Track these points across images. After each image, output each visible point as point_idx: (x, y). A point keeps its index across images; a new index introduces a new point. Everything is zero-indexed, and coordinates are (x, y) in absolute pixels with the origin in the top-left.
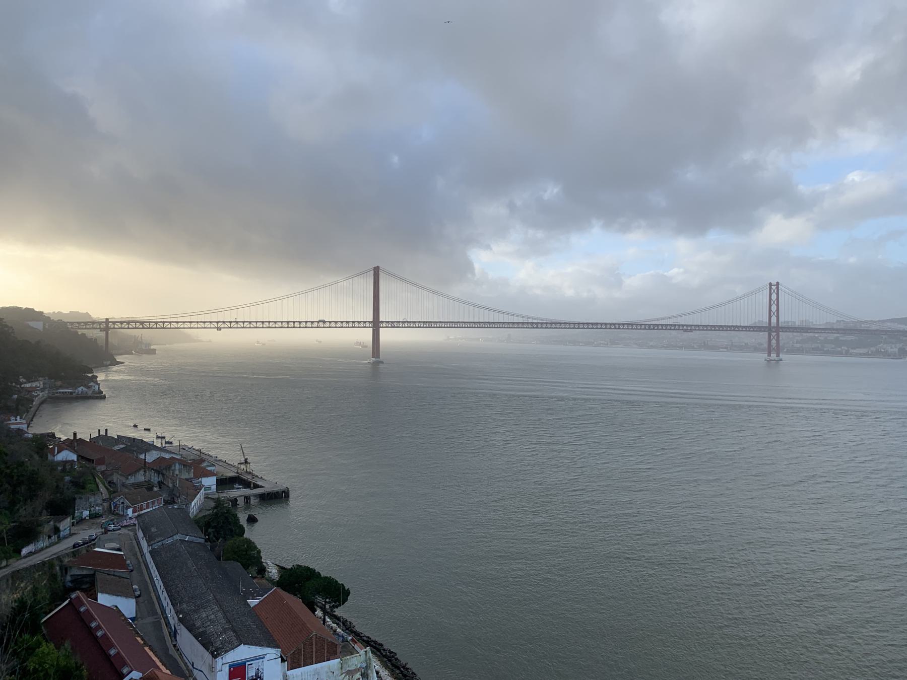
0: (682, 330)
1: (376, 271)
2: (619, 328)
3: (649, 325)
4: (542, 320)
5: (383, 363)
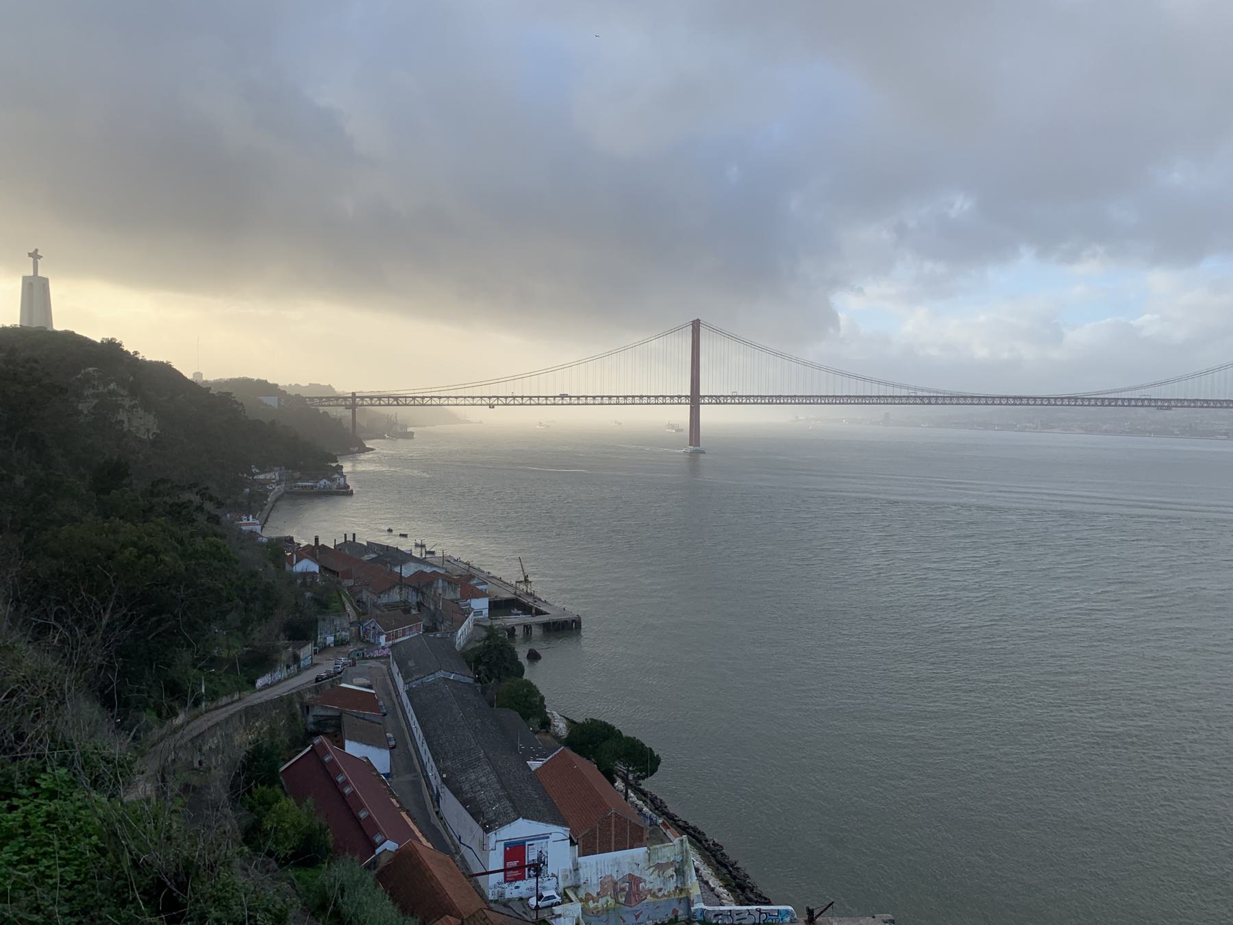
0: (1155, 406)
1: (696, 326)
2: (1055, 405)
3: (1103, 399)
4: (937, 392)
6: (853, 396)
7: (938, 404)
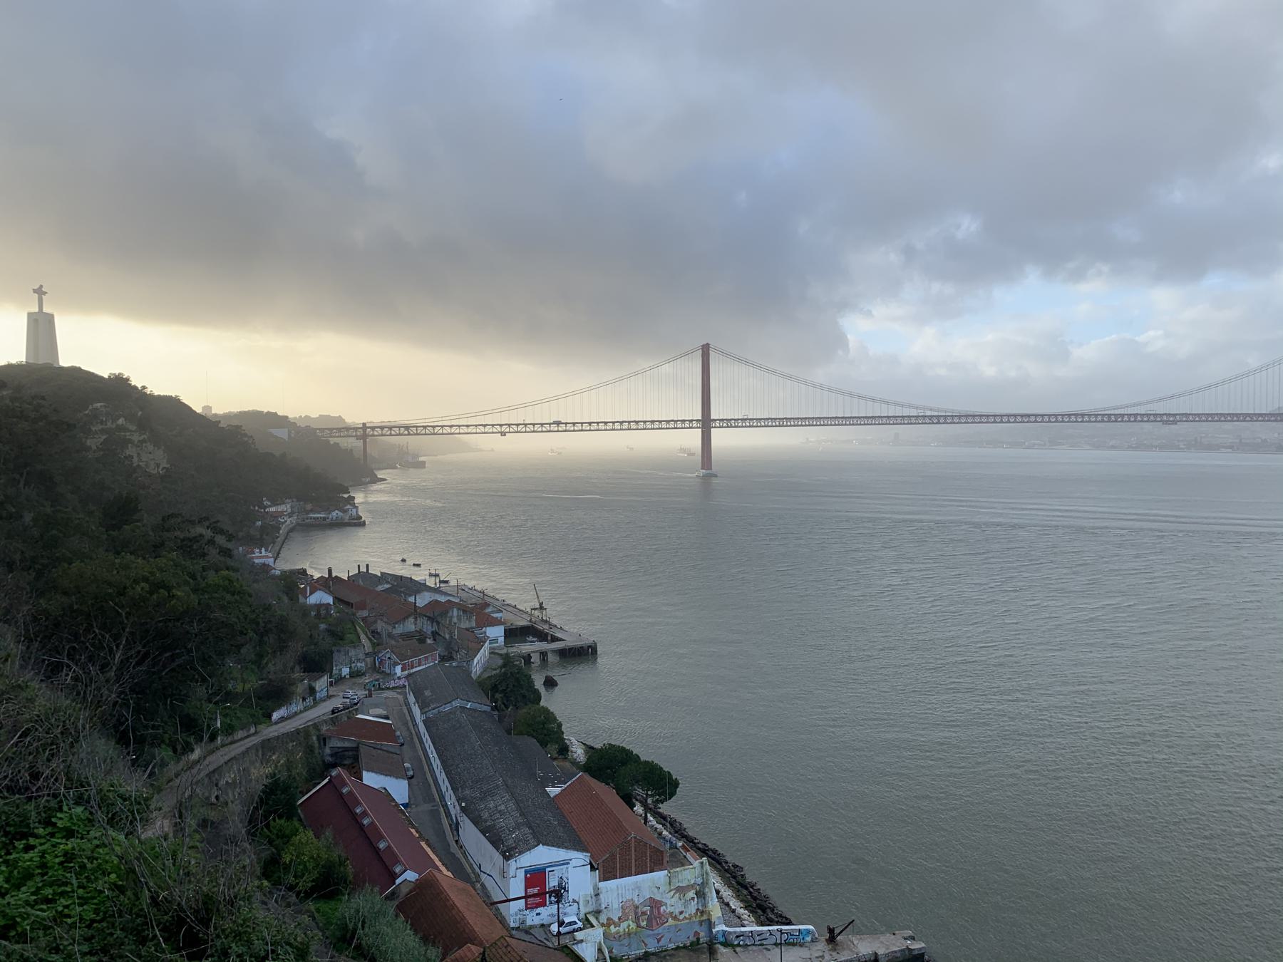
1: (706, 350)
2: (1063, 421)
3: (1109, 415)
5: (716, 476)
6: (863, 417)
7: (947, 423)
